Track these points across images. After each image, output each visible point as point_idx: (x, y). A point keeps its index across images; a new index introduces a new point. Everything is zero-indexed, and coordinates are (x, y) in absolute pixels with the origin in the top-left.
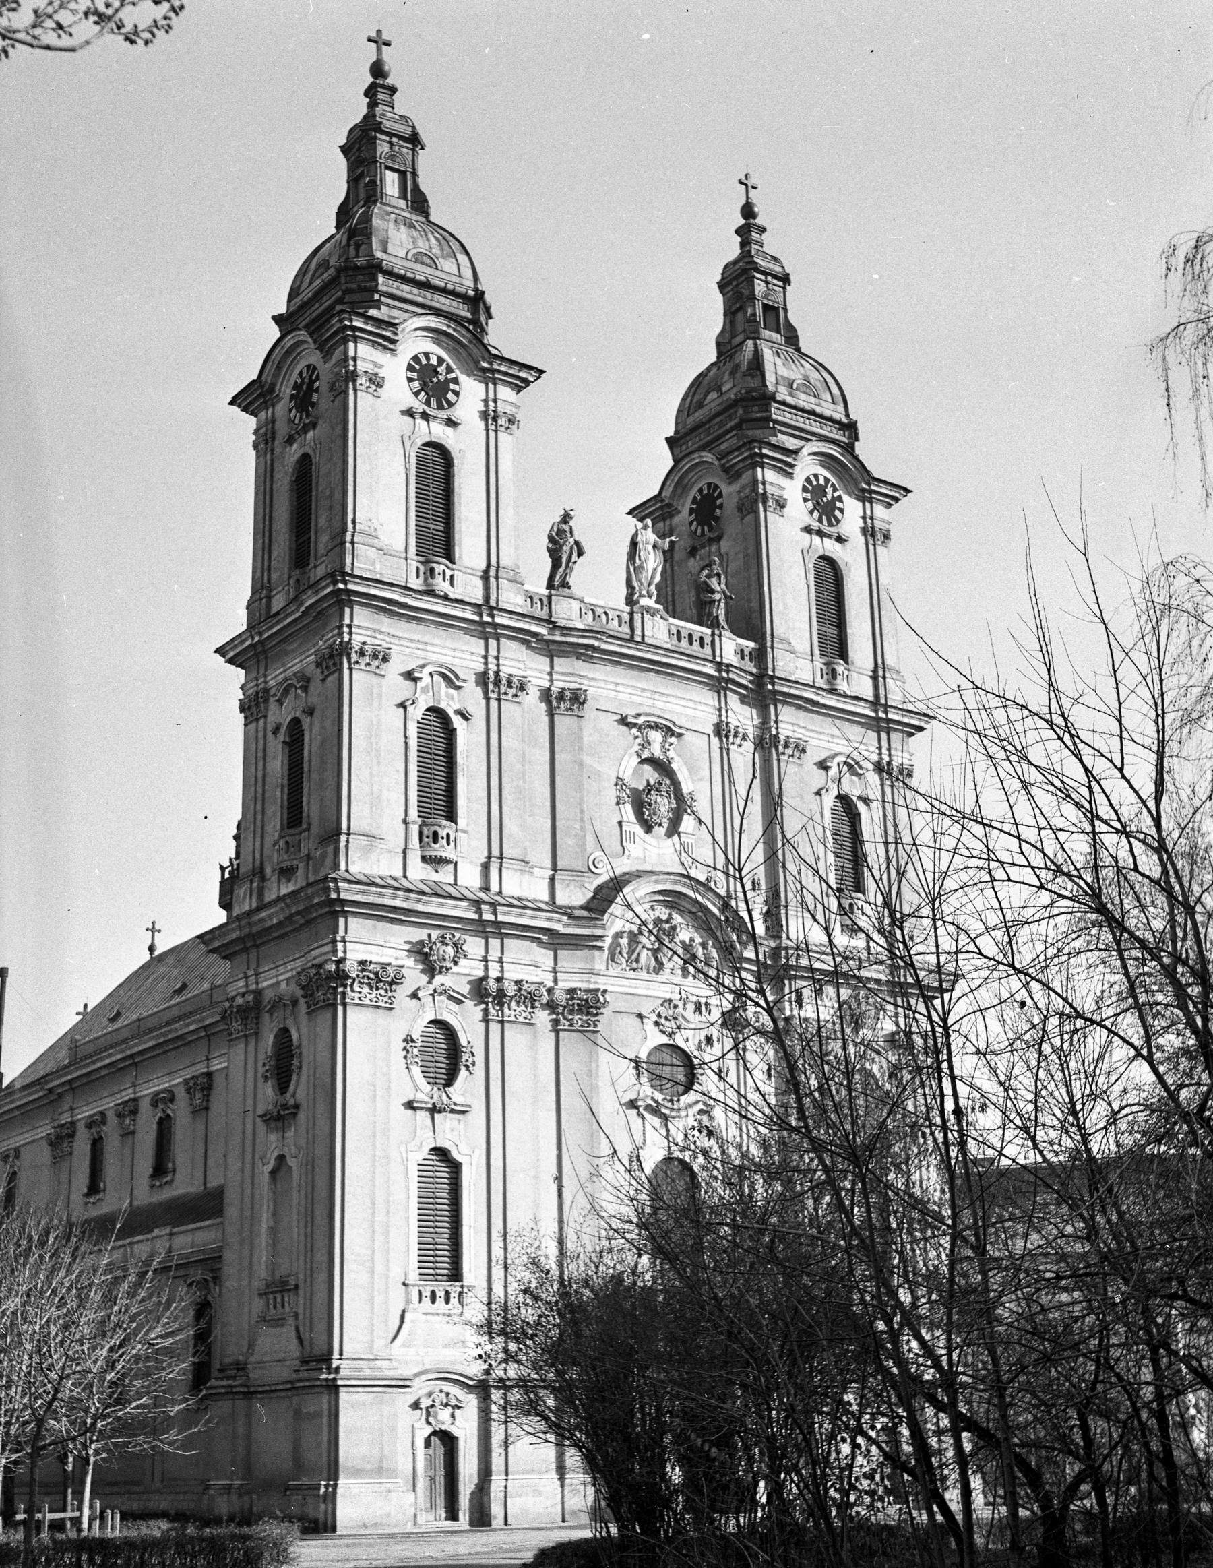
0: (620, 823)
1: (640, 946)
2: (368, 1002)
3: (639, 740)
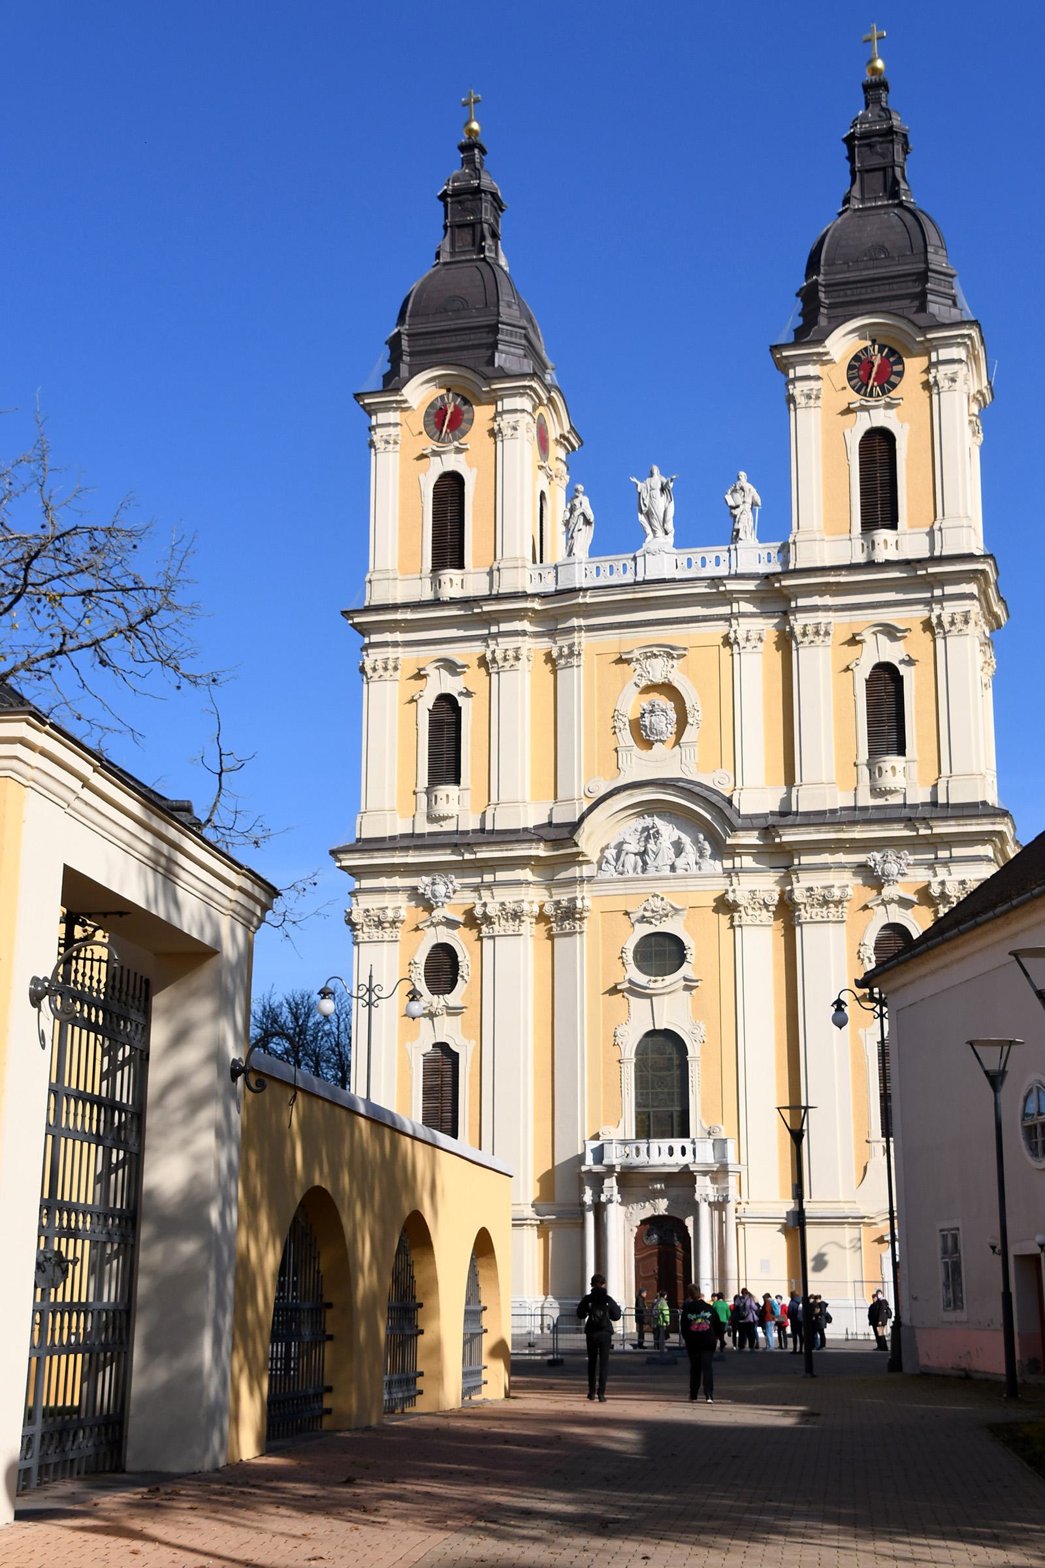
0: (616, 750)
1: (624, 853)
2: (376, 939)
3: (638, 672)
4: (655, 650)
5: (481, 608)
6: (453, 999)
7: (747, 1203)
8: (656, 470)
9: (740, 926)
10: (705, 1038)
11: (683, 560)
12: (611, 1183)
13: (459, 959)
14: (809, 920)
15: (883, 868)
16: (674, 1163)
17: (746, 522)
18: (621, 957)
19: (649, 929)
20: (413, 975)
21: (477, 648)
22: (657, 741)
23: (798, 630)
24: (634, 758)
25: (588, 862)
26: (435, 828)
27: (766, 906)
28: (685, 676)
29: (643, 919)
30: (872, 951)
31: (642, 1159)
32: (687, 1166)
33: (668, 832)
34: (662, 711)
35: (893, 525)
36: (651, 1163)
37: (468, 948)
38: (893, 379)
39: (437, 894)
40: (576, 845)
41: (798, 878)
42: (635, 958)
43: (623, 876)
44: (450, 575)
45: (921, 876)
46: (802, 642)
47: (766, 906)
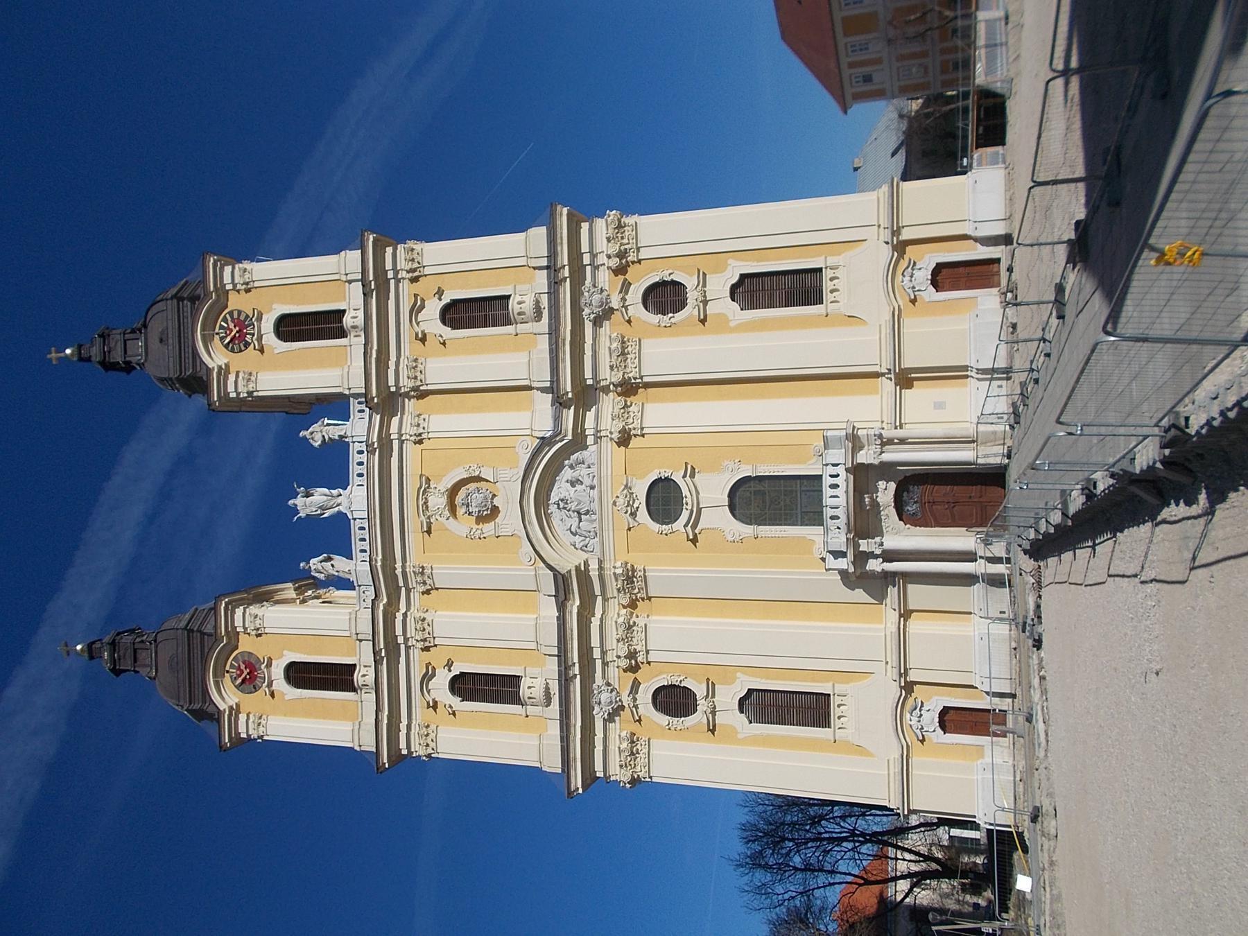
0: (497, 537)
2: (647, 759)
4: (421, 503)
5: (381, 649)
6: (700, 690)
7: (882, 422)
8: (291, 502)
9: (642, 429)
10: (736, 461)
11: (358, 480)
12: (864, 545)
13: (666, 684)
14: (637, 369)
15: (596, 307)
16: (845, 483)
18: (666, 535)
19: (643, 508)
20: (679, 728)
21: (416, 654)
22: (492, 502)
23: (411, 384)
24: (503, 523)
25: (586, 563)
26: (556, 700)
27: (626, 406)
28: (444, 479)
29: (633, 514)
30: (665, 317)
31: (840, 512)
32: (847, 470)
33: (561, 490)
34: (467, 497)
36: (845, 505)
37: (657, 676)
38: (242, 318)
39: (609, 700)
40: (570, 571)
41: (603, 380)
42: (667, 524)
43: (598, 532)
44: (358, 678)
45: (604, 277)
46: (421, 381)
47: (626, 406)
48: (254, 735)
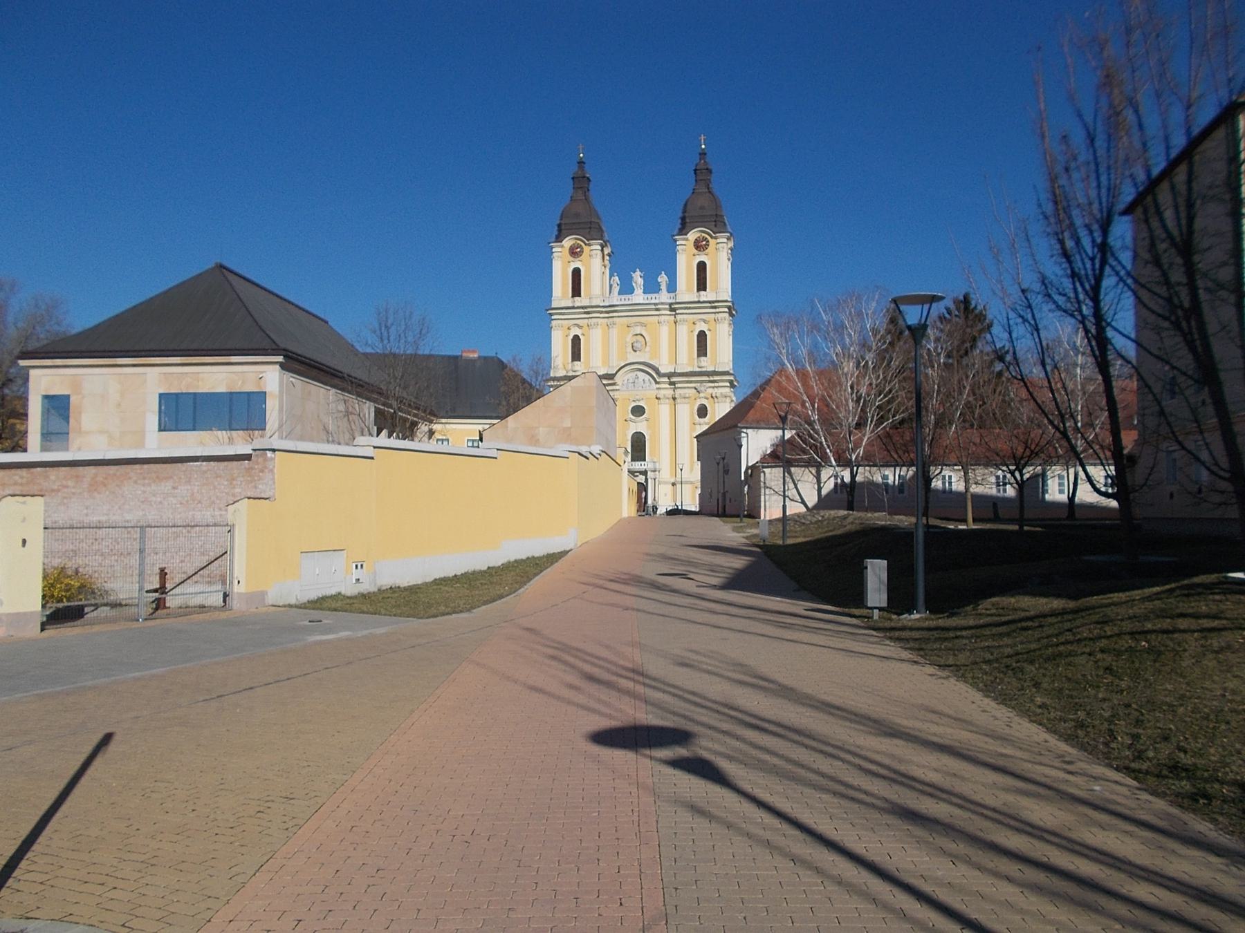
17: (664, 287)
35: (705, 290)
48: (555, 254)
